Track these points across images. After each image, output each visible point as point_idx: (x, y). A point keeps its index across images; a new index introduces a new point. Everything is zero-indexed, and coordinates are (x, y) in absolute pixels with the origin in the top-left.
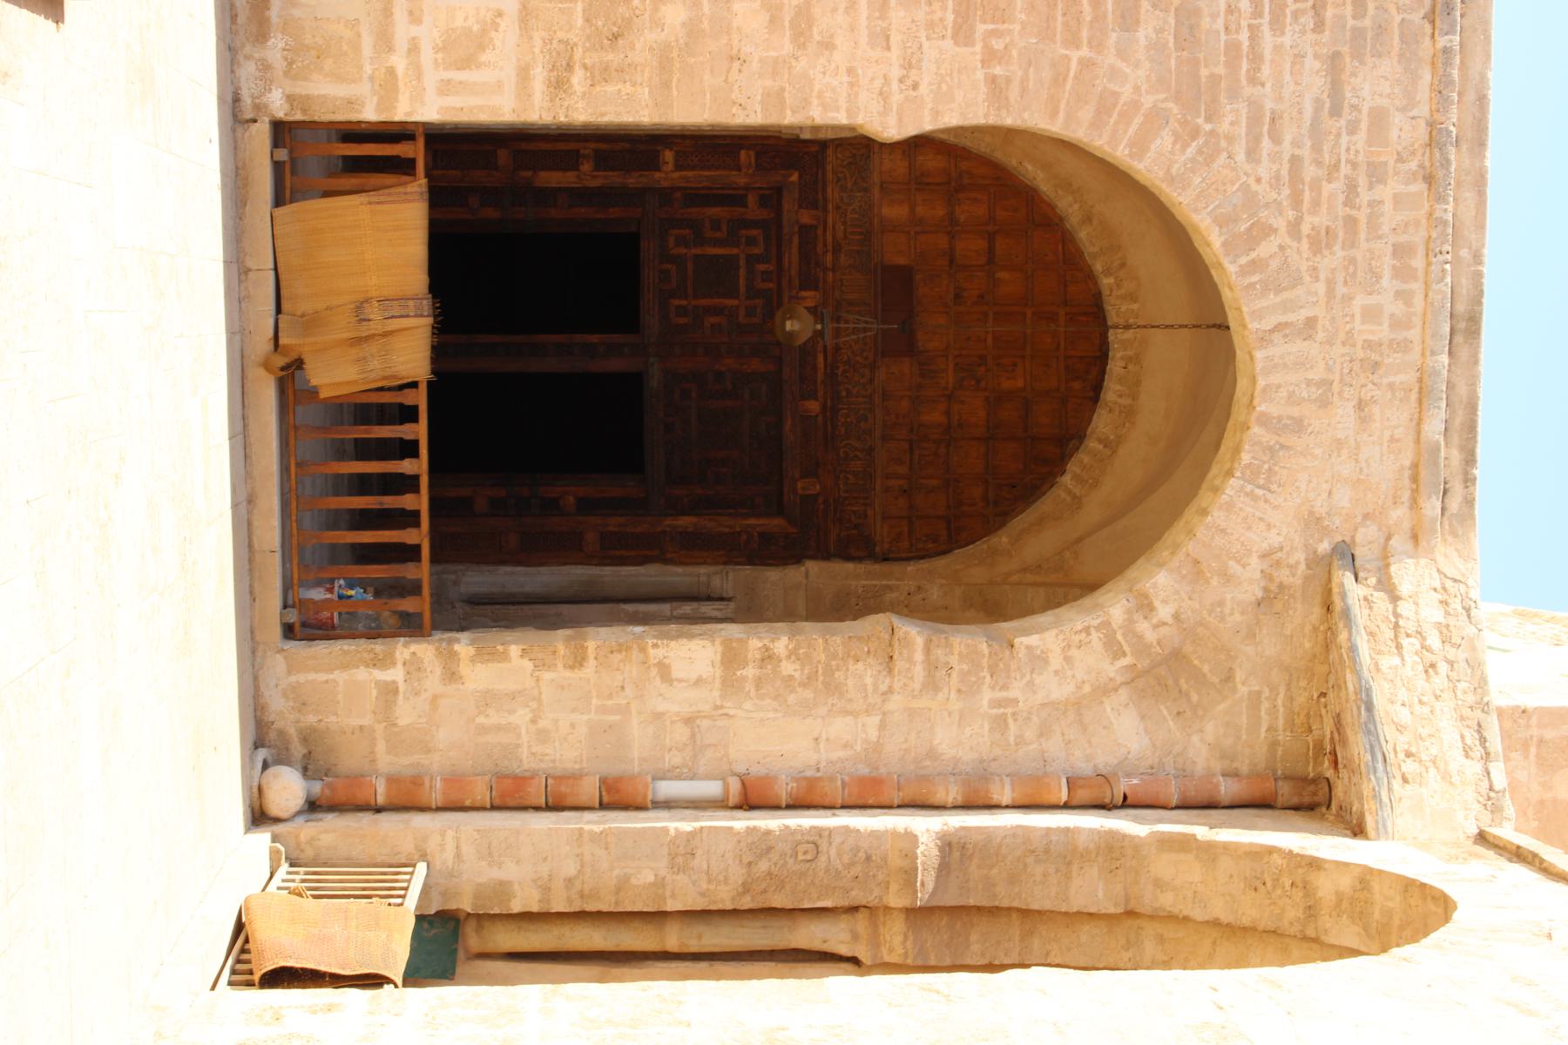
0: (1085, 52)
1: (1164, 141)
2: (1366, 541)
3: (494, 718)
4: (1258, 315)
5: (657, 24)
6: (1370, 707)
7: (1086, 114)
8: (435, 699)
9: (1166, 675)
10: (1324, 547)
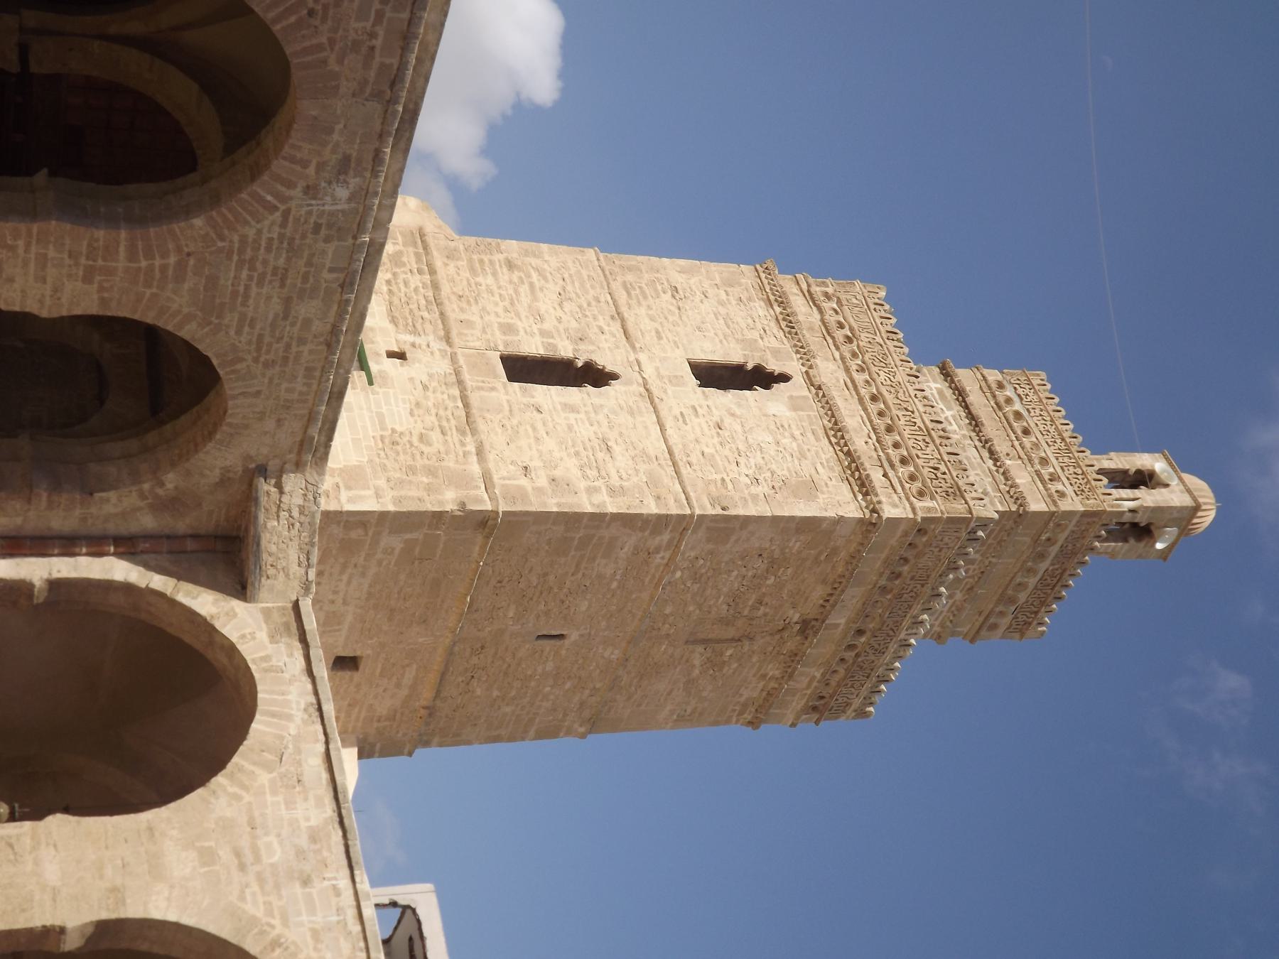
0: (154, 290)
1: (193, 326)
2: (273, 465)
6: (258, 545)
10: (253, 466)
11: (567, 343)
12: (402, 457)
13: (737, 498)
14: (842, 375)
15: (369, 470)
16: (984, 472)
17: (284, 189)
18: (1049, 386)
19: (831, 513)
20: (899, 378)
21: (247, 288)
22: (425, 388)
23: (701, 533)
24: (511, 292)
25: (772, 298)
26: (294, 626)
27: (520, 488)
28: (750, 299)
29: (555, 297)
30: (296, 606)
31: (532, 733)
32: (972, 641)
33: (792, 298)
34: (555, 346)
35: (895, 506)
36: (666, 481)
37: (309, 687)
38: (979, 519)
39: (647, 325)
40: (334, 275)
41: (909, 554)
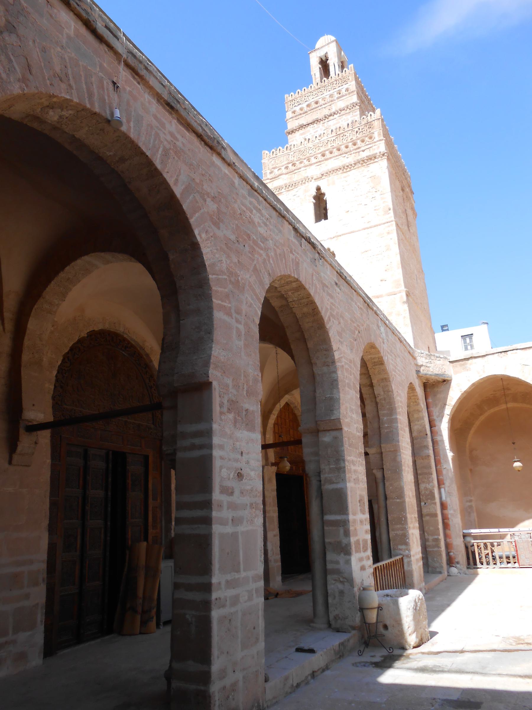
16: (340, 119)
20: (311, 146)
26: (463, 362)
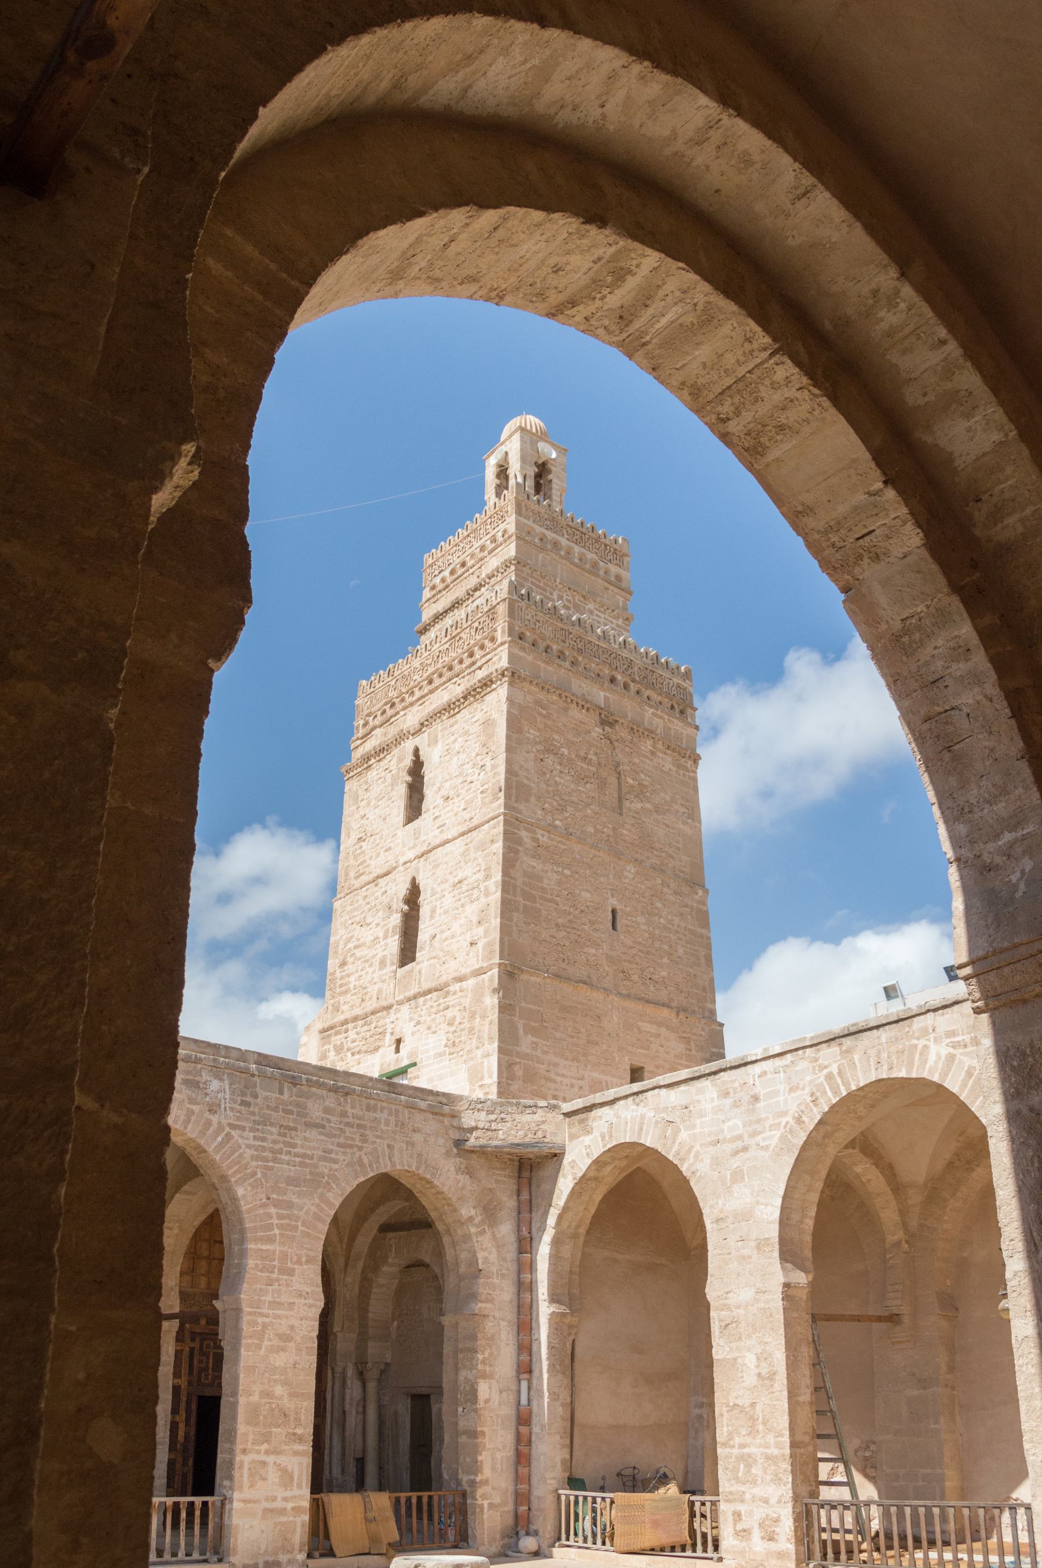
0: (299, 1224)
1: (330, 1195)
2: (455, 1135)
3: (499, 1466)
4: (386, 1166)
5: (281, 1398)
7: (320, 1226)
8: (493, 1488)
9: (490, 1213)
10: (455, 1150)
11: (392, 918)
12: (463, 1038)
13: (494, 781)
14: (415, 708)
15: (471, 1063)
17: (211, 1129)
18: (434, 551)
19: (504, 707)
21: (297, 1155)
22: (418, 1023)
23: (521, 807)
24: (360, 962)
25: (365, 766)
27: (484, 948)
28: (366, 782)
29: (363, 929)
30: (568, 1115)
31: (704, 931)
32: (630, 593)
33: (366, 750)
34: (394, 927)
35: (500, 658)
36: (481, 836)
37: (622, 1102)
38: (509, 593)
39: (381, 859)
40: (286, 1090)
41: (542, 645)
